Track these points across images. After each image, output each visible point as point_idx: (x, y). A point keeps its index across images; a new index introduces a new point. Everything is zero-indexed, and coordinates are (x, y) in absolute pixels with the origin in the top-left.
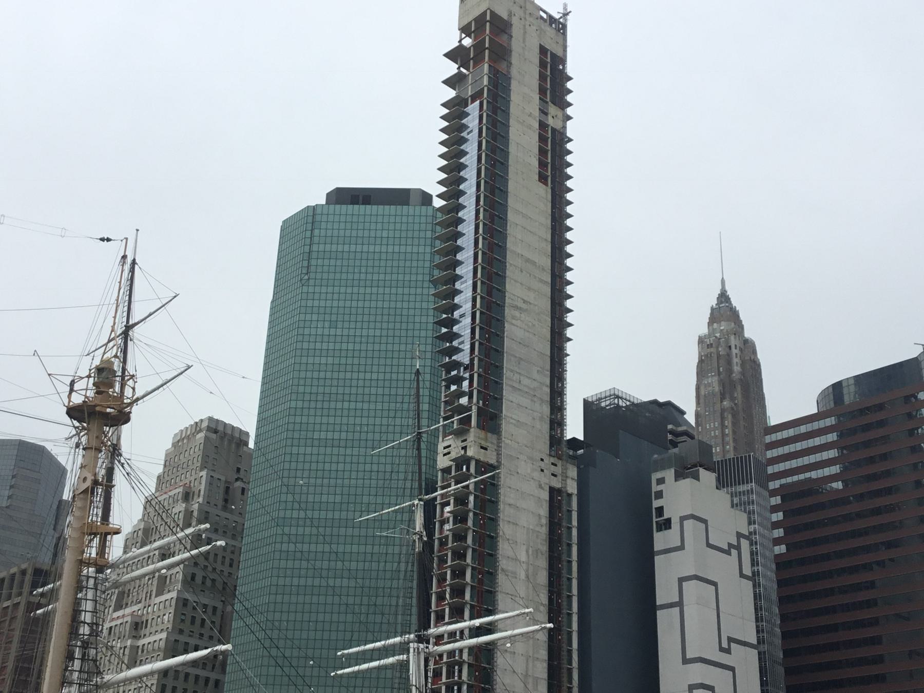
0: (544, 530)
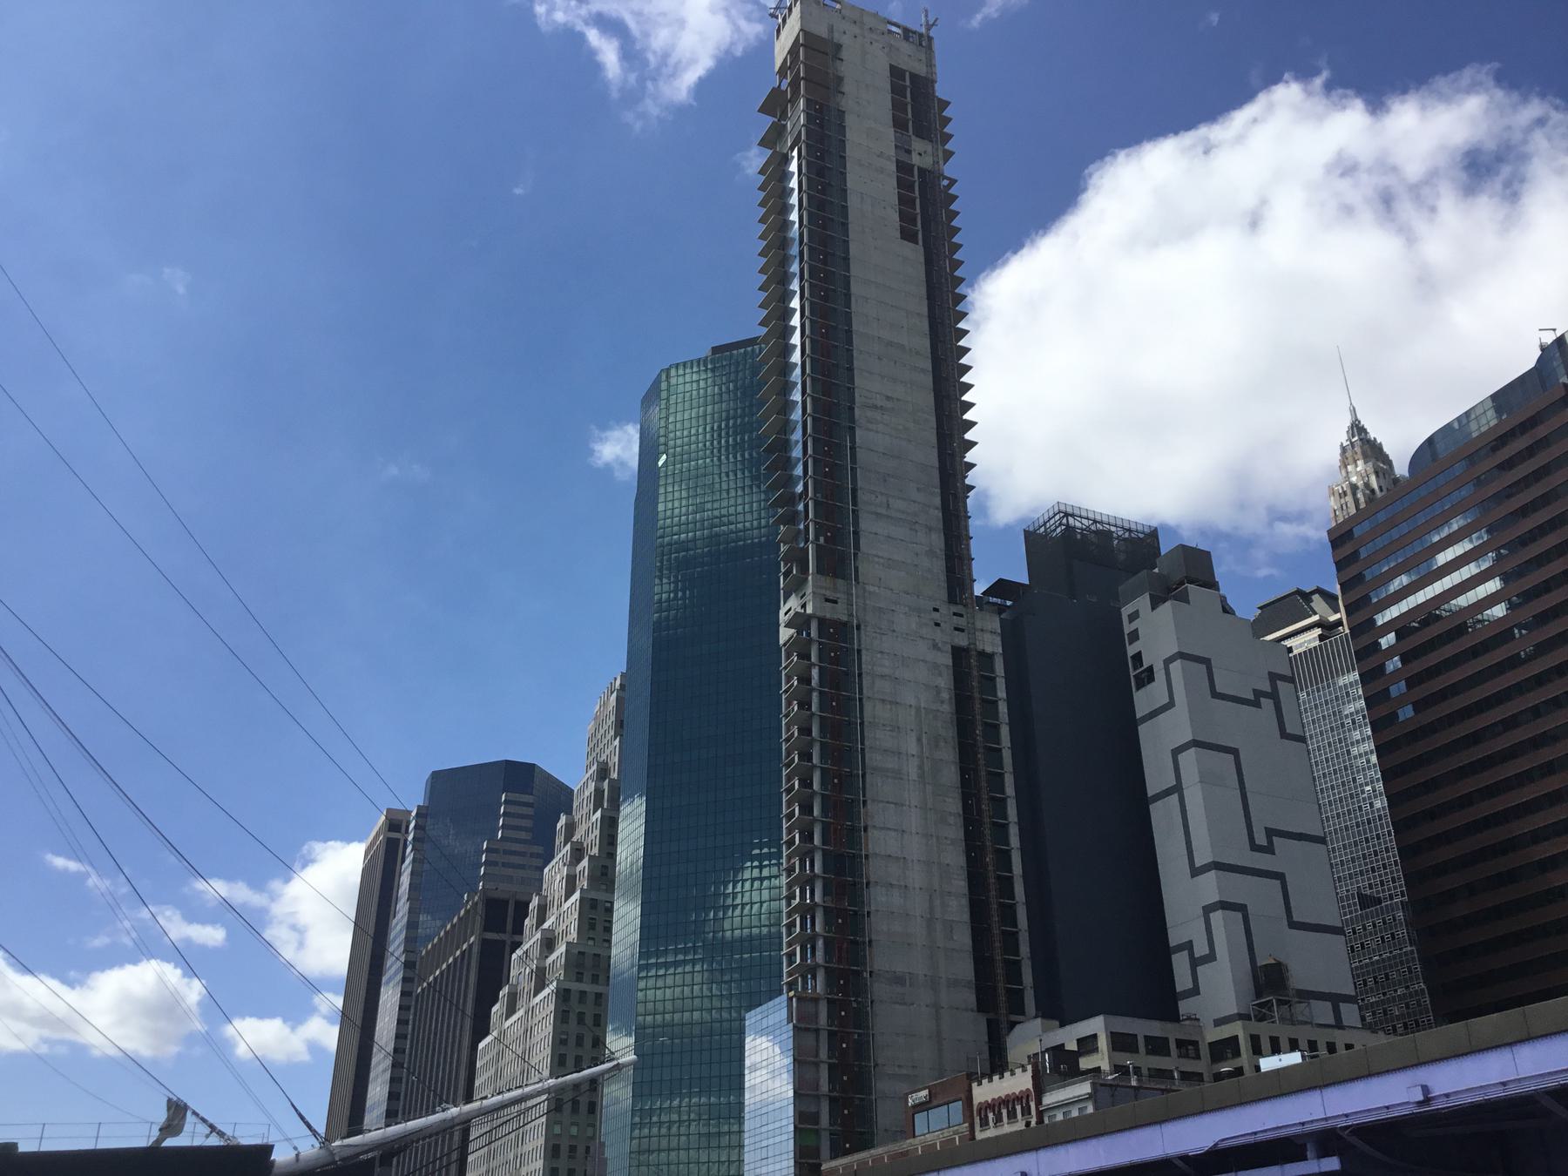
0: (947, 708)
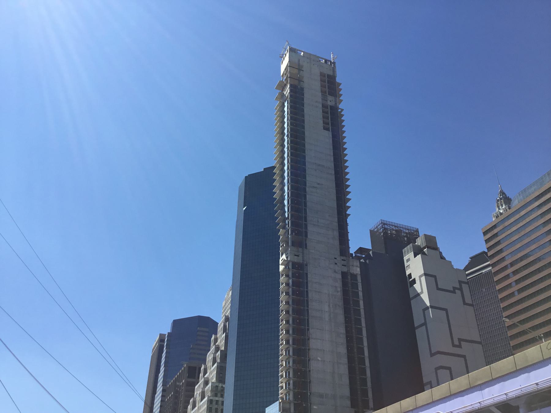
0: (340, 294)
